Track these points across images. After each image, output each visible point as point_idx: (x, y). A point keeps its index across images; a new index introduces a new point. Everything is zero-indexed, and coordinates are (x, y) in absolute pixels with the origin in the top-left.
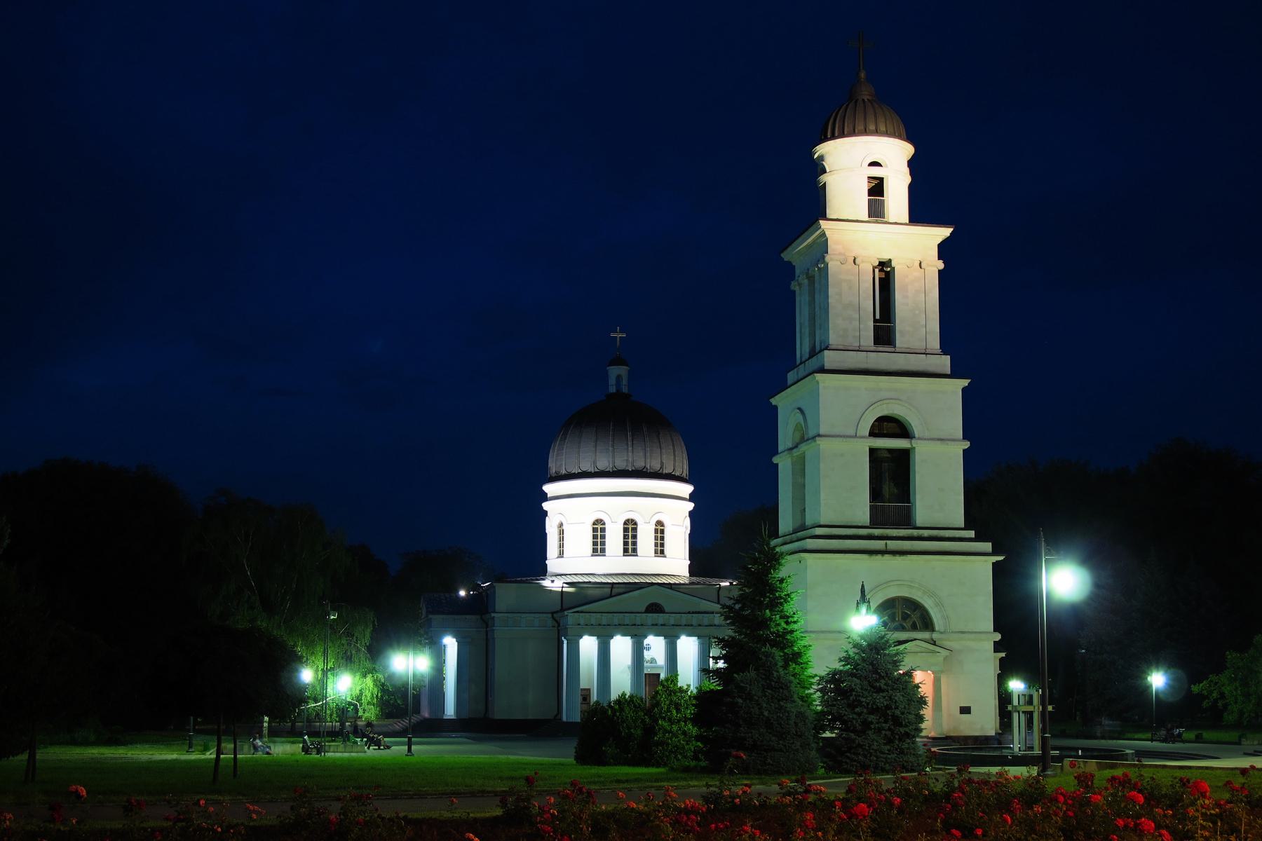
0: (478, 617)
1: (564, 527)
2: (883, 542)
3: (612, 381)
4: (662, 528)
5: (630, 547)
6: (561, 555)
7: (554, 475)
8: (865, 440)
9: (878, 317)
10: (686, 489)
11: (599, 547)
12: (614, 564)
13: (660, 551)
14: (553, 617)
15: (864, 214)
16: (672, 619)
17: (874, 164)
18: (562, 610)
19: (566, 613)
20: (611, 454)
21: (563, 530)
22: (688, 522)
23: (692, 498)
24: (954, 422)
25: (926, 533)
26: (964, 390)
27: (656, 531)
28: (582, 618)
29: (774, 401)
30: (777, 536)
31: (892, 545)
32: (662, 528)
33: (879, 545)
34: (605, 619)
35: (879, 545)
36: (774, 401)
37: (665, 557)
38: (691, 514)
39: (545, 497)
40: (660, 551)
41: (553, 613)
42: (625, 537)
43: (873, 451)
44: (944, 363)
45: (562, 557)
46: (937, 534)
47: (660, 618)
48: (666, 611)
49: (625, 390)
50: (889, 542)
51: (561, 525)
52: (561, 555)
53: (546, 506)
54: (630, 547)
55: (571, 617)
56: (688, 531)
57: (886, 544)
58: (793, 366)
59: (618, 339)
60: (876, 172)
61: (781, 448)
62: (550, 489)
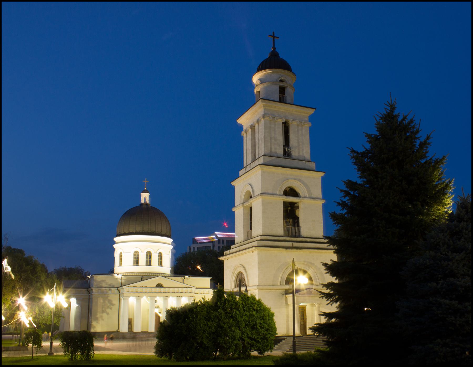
0: (86, 289)
1: (122, 254)
2: (291, 243)
3: (143, 199)
4: (161, 255)
5: (149, 262)
6: (120, 265)
7: (118, 234)
8: (280, 196)
9: (284, 145)
10: (170, 240)
11: (136, 262)
12: (142, 268)
13: (160, 264)
14: (117, 289)
15: (278, 100)
16: (167, 290)
17: (281, 81)
18: (121, 286)
19: (123, 287)
20: (142, 226)
21: (122, 256)
24: (318, 191)
25: (308, 240)
26: (322, 178)
27: (159, 256)
28: (130, 289)
29: (233, 183)
31: (296, 244)
32: (161, 255)
33: (289, 244)
34: (139, 290)
35: (289, 244)
36: (233, 183)
37: (162, 266)
39: (114, 243)
40: (160, 264)
41: (117, 288)
42: (147, 258)
43: (285, 203)
45: (121, 266)
46: (313, 240)
47: (162, 289)
48: (164, 287)
49: (148, 202)
50: (294, 243)
51: (121, 253)
52: (120, 265)
54: (149, 262)
55: (125, 289)
57: (292, 244)
58: (242, 168)
59: (146, 183)
60: (283, 84)
61: (236, 204)
62: (116, 239)
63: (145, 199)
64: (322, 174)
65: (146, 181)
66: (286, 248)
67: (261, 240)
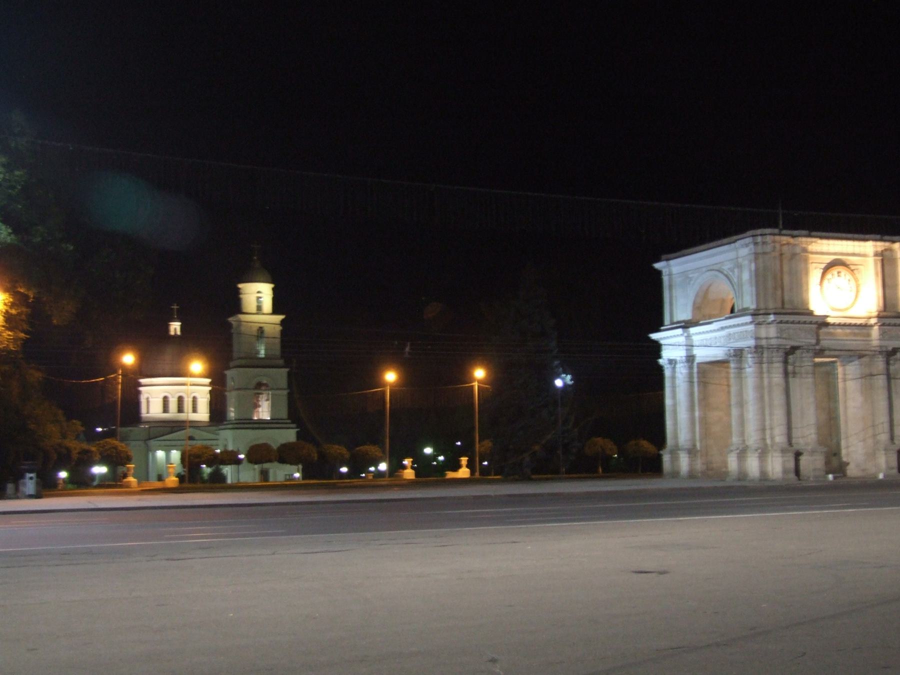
5: (180, 409)
10: (208, 381)
11: (166, 409)
13: (195, 410)
17: (259, 292)
22: (209, 396)
23: (211, 384)
30: (226, 421)
34: (168, 443)
38: (211, 392)
44: (281, 362)
52: (148, 413)
53: (141, 389)
54: (180, 409)
55: (152, 443)
56: (209, 400)
60: (259, 295)
62: (143, 381)
63: (175, 329)
64: (287, 370)
65: (175, 307)
66: (253, 428)
67: (237, 424)
